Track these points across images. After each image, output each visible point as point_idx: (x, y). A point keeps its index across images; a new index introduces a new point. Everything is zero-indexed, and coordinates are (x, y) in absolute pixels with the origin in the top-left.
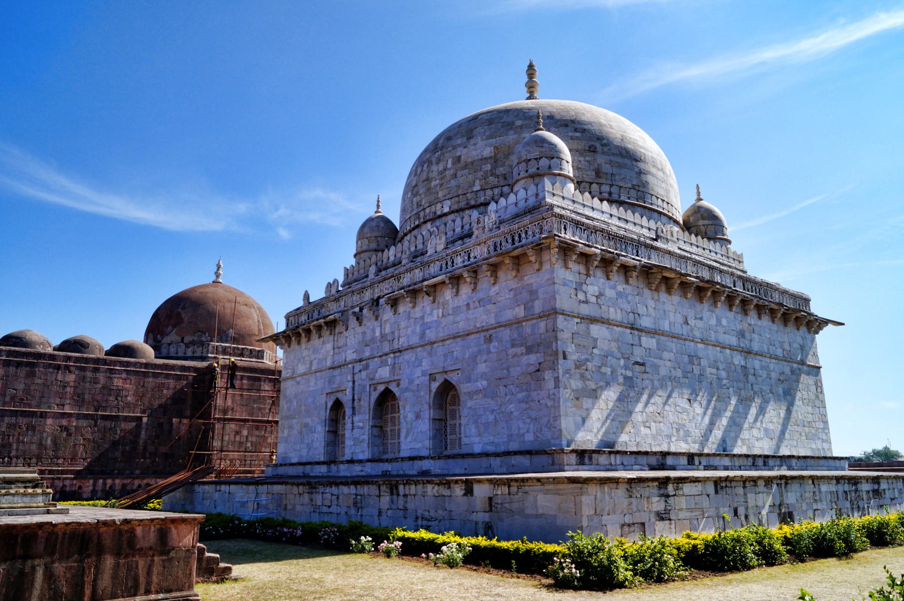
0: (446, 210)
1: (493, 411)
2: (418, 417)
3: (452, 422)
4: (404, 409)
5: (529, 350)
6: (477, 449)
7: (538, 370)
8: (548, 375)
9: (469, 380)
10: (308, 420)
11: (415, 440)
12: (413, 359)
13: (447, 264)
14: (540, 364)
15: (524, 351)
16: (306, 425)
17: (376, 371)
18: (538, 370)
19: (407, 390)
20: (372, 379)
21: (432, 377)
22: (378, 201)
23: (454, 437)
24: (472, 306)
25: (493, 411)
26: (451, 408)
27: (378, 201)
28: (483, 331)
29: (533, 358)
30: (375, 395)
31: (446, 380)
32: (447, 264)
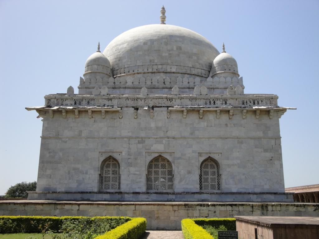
0: (174, 70)
1: (244, 174)
2: (189, 172)
3: (206, 177)
4: (178, 168)
5: (266, 151)
6: (234, 190)
7: (271, 160)
8: (276, 162)
9: (228, 159)
10: (79, 166)
11: (187, 184)
12: (185, 143)
13: (210, 102)
14: (272, 157)
15: (263, 151)
16: (74, 169)
17: (152, 146)
18: (271, 160)
19: (179, 158)
20: (148, 149)
21: (200, 154)
22: (99, 46)
23: (206, 183)
24: (229, 125)
25: (244, 174)
26: (205, 170)
27: (99, 46)
28: (237, 138)
29: (268, 155)
30: (150, 158)
31: (209, 157)
32: (210, 102)
